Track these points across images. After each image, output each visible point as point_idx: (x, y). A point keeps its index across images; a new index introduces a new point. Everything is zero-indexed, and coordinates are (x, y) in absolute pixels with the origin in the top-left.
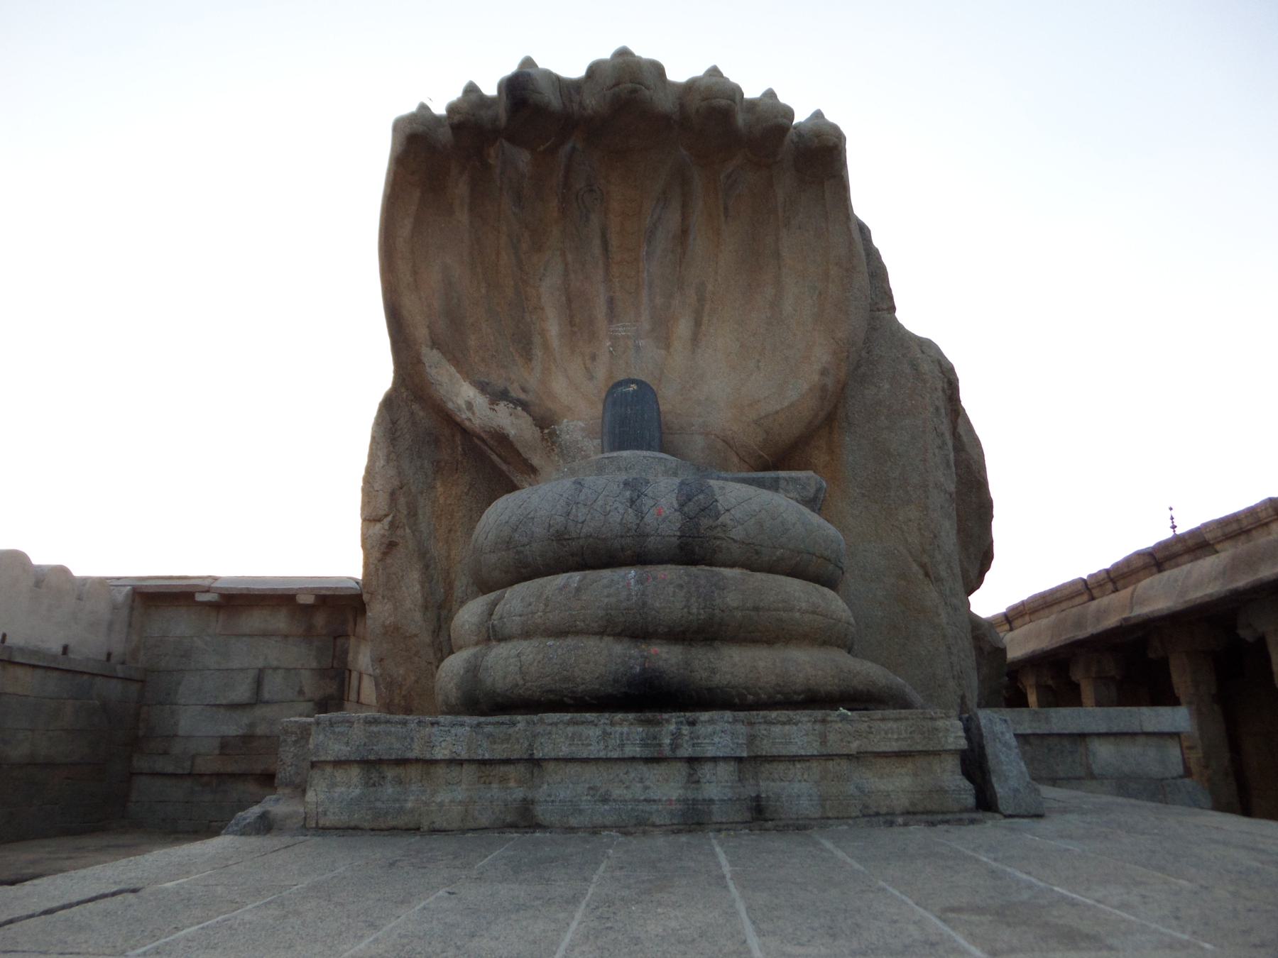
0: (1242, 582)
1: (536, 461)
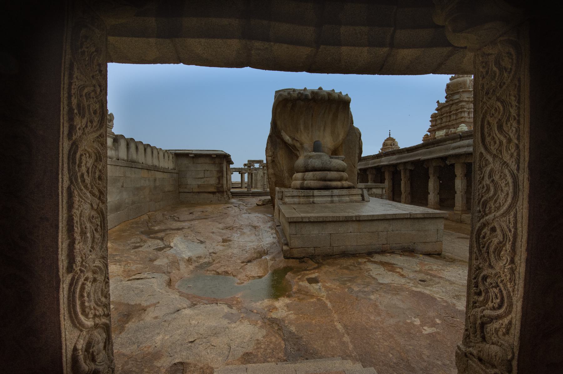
0: (399, 162)
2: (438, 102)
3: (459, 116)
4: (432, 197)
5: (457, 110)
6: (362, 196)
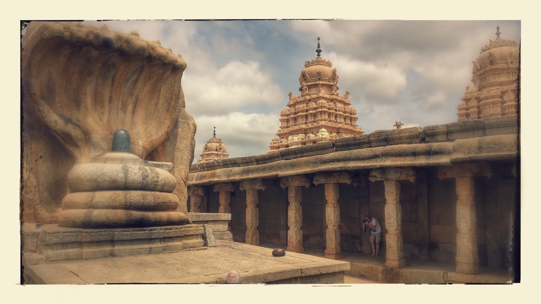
0: (244, 177)
1: (80, 144)
2: (290, 95)
3: (319, 118)
4: (294, 234)
6: (204, 237)
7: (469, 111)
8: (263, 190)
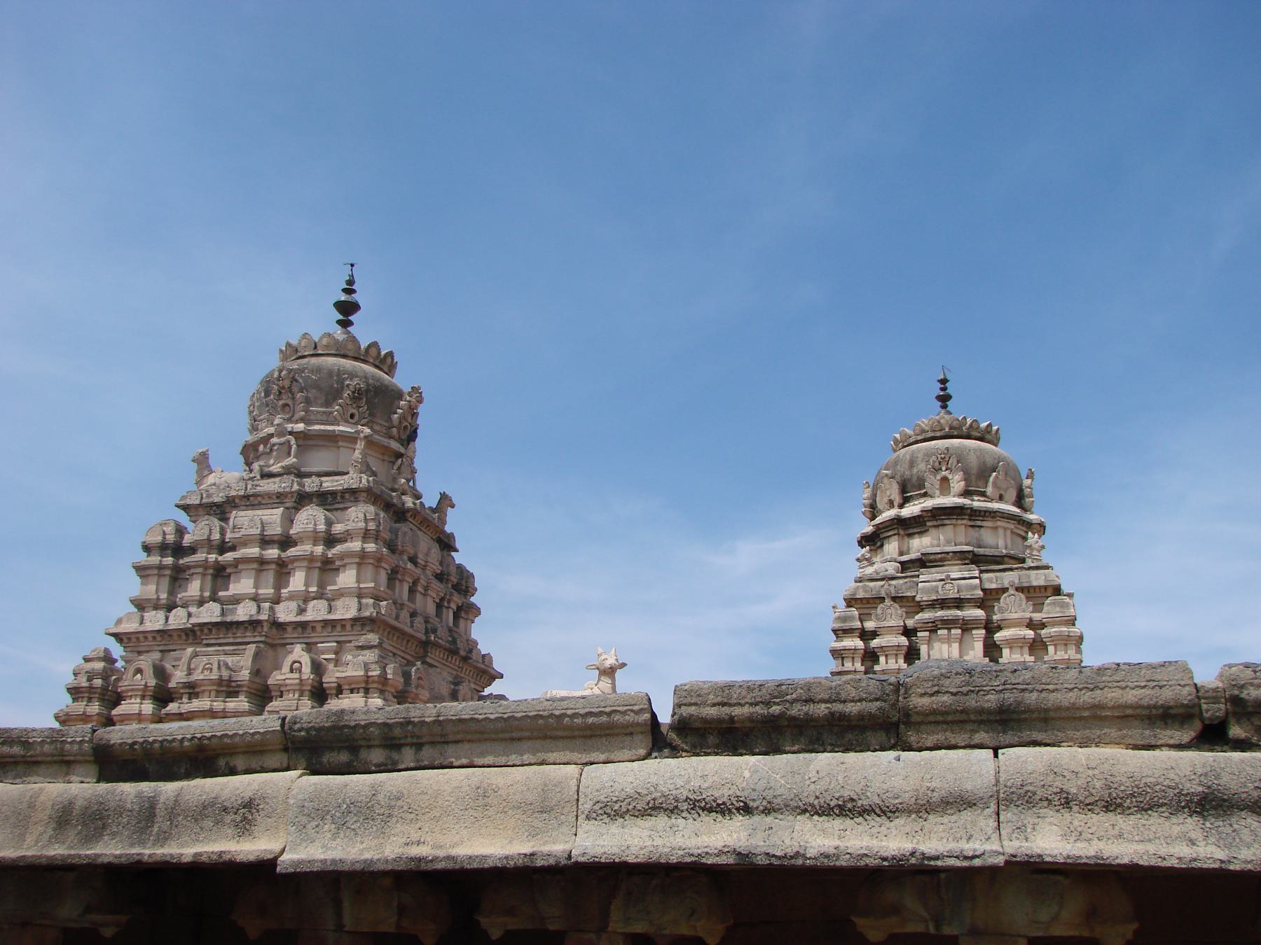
2: (202, 461)
3: (347, 579)
5: (331, 541)
7: (875, 643)
8: (108, 932)
